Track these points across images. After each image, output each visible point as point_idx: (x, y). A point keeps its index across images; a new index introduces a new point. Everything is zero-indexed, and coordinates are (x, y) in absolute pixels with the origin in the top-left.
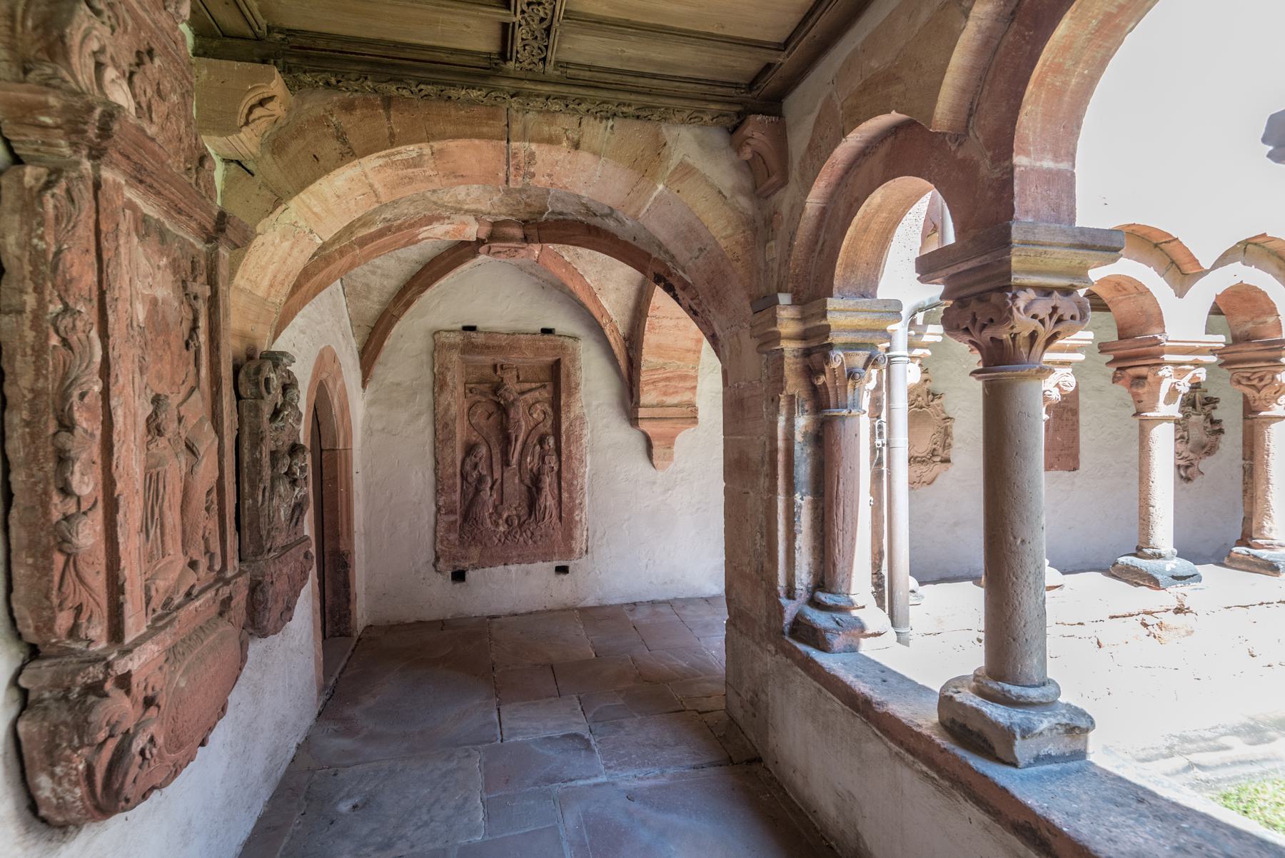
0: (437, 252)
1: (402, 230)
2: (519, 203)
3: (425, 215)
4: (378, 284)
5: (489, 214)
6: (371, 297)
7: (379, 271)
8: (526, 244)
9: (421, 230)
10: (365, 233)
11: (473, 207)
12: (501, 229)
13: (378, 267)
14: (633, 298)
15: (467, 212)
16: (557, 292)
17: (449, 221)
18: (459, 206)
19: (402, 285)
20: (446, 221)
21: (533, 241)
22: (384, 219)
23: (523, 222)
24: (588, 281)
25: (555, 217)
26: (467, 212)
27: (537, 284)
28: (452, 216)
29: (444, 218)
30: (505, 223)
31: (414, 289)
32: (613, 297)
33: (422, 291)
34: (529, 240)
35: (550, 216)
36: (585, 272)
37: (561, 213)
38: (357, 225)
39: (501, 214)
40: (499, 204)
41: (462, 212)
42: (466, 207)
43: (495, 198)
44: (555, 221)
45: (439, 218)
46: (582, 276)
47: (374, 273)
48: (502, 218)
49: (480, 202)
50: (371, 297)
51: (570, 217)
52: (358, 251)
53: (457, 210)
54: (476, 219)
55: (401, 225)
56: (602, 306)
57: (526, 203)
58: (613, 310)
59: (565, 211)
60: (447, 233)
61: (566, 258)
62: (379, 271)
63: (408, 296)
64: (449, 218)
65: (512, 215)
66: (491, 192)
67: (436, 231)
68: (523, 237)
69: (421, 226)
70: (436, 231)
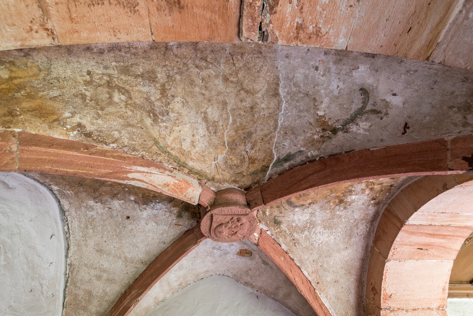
0: (163, 247)
1: (105, 156)
2: (243, 161)
3: (143, 157)
4: (101, 291)
5: (213, 179)
6: (90, 307)
7: (105, 276)
8: (249, 210)
9: (134, 168)
10: (41, 133)
11: (197, 166)
12: (224, 196)
13: (105, 271)
14: (353, 291)
15: (191, 172)
16: (270, 300)
17: (170, 174)
18: (183, 159)
19: (123, 291)
20: (167, 172)
21: (256, 205)
22: (79, 125)
23: (246, 189)
24: (306, 273)
25: (279, 169)
26: (191, 172)
27: (252, 293)
28: (175, 171)
29: (165, 169)
30: (228, 190)
31: (133, 292)
32: (332, 291)
33: (139, 294)
34: (252, 205)
35: (275, 169)
36: (301, 261)
37: (288, 158)
38: (25, 105)
39: (225, 181)
40: (223, 167)
41: (186, 171)
42: (190, 164)
43: (220, 157)
44: (280, 174)
45: (159, 166)
46: (299, 268)
47: (99, 278)
48: (226, 186)
49: (205, 161)
50: (90, 307)
51: (299, 159)
52: (14, 148)
53: (181, 166)
54: (200, 184)
55: (107, 151)
56: (322, 304)
57: (250, 159)
58: (335, 310)
59: (293, 150)
60: (167, 185)
61: (283, 246)
62: (105, 276)
63: (126, 302)
64: (171, 172)
65: (235, 181)
66: (216, 148)
67: (153, 178)
68: (246, 203)
69: (134, 164)
70: (153, 178)
